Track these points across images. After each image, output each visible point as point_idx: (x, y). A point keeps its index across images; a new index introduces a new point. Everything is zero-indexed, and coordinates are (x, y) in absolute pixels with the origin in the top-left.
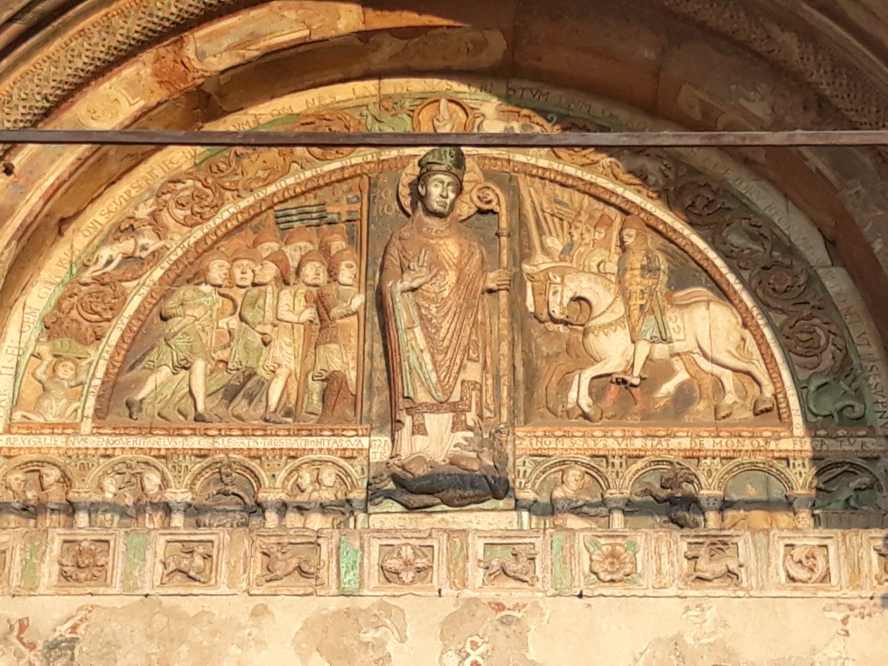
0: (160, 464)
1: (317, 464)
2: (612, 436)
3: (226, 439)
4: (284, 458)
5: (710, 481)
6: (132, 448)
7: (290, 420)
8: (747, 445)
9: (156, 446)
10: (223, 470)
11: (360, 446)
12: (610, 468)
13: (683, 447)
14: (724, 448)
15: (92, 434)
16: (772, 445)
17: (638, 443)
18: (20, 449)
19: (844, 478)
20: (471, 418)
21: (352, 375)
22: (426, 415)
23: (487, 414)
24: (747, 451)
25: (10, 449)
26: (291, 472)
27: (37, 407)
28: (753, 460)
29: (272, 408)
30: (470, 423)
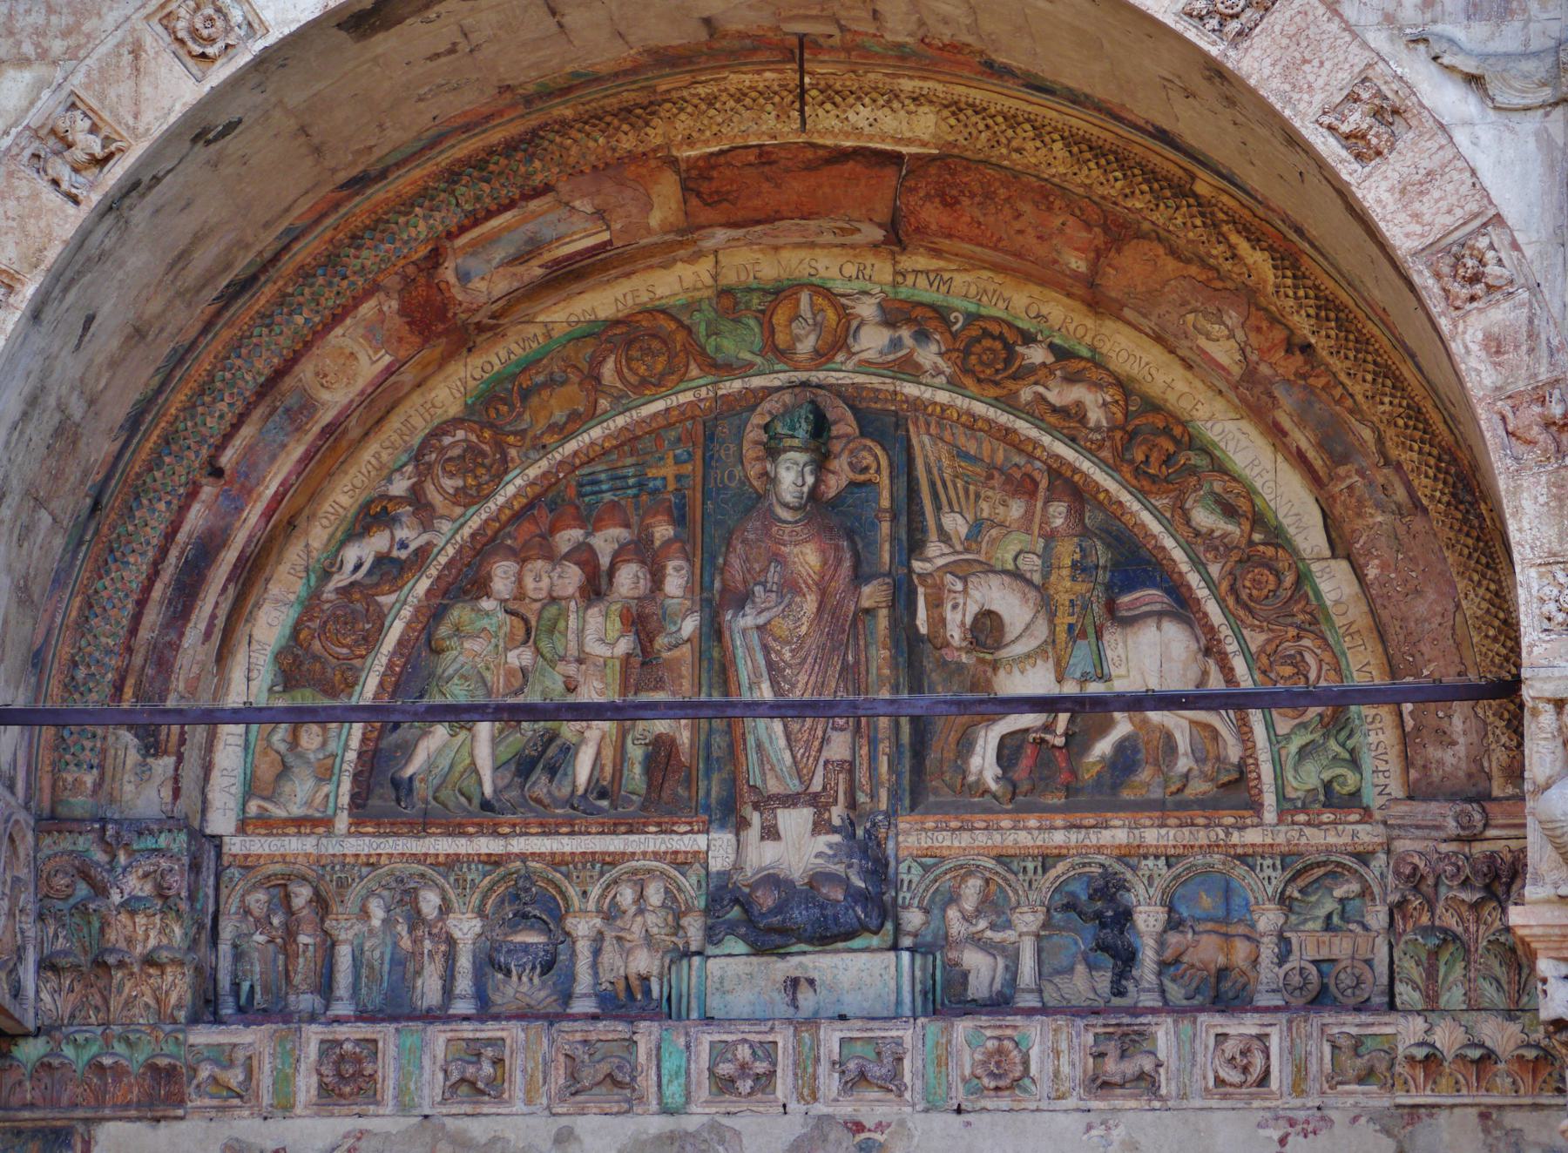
2: (1025, 828)
3: (522, 839)
4: (598, 866)
5: (1151, 891)
6: (403, 854)
7: (605, 803)
8: (1202, 837)
9: (432, 851)
10: (521, 884)
11: (696, 848)
12: (1021, 876)
13: (1117, 842)
14: (1171, 843)
15: (350, 834)
17: (1059, 838)
18: (260, 856)
19: (1328, 882)
20: (837, 814)
22: (779, 811)
23: (862, 798)
24: (1201, 847)
25: (246, 857)
26: (608, 886)
28: (1209, 859)
30: (836, 822)
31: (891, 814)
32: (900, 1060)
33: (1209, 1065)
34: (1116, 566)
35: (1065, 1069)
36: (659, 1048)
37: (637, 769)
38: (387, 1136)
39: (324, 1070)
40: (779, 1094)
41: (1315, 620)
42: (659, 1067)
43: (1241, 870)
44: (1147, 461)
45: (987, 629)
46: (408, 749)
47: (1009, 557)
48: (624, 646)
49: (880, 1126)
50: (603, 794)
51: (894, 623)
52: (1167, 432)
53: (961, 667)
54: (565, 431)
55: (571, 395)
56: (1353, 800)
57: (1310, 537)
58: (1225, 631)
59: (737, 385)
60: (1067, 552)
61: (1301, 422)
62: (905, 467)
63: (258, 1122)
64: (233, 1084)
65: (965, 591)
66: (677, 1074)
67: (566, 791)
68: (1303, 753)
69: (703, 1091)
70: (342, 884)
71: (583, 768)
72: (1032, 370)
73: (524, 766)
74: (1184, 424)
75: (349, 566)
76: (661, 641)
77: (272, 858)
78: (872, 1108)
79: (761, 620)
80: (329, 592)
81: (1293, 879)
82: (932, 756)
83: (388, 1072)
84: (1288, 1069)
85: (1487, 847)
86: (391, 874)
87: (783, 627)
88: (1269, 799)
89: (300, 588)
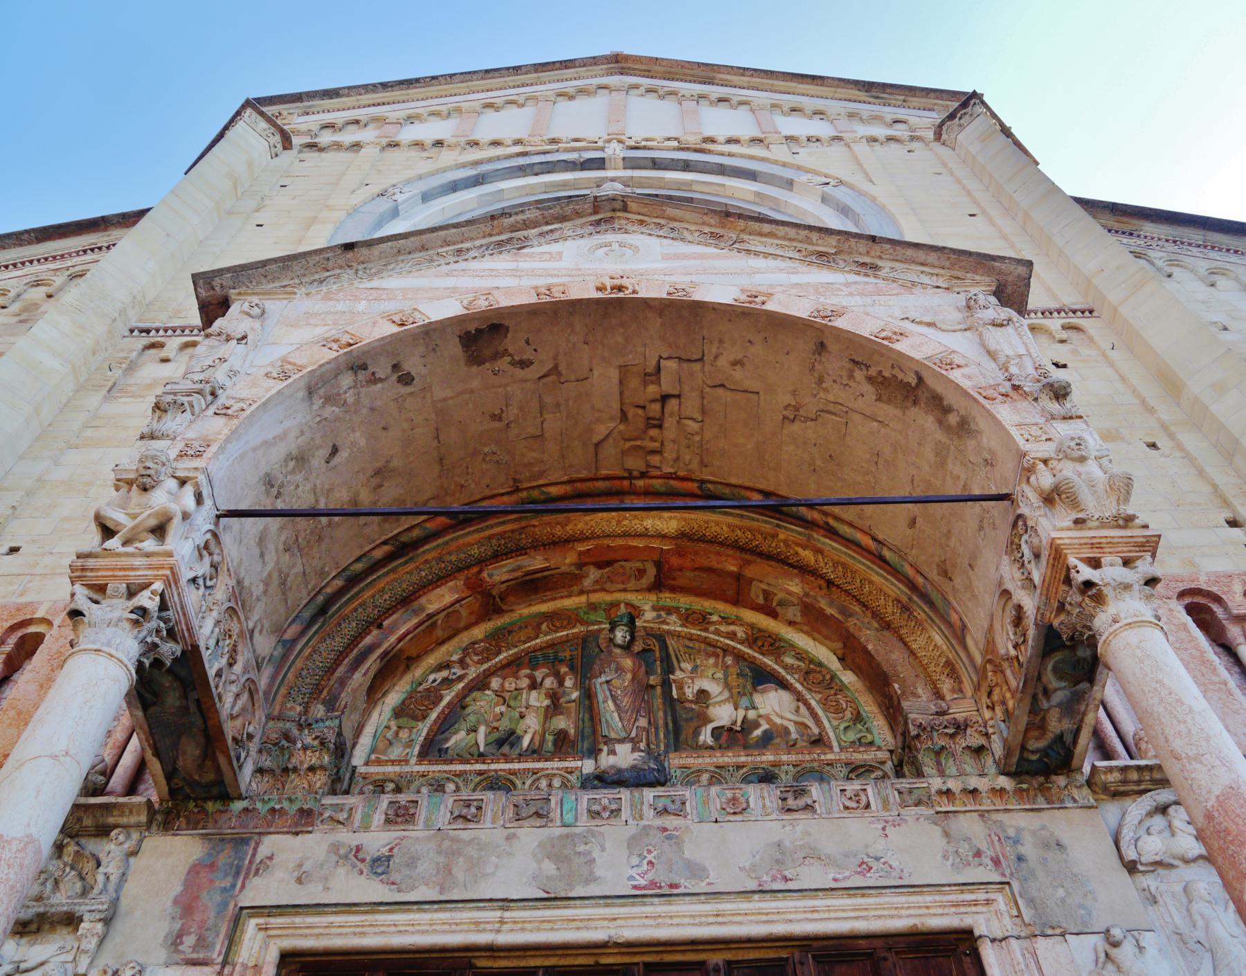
0: (456, 779)
1: (550, 777)
8: (807, 757)
16: (823, 757)
17: (743, 759)
20: (642, 746)
21: (572, 731)
23: (652, 746)
27: (384, 752)
29: (524, 749)
30: (642, 748)
31: (666, 752)
32: (684, 803)
33: (838, 801)
34: (754, 678)
35: (768, 804)
36: (562, 800)
37: (550, 744)
38: (418, 838)
39: (389, 812)
40: (624, 818)
41: (842, 688)
42: (561, 808)
43: (828, 768)
44: (763, 646)
45: (703, 694)
46: (447, 740)
47: (710, 675)
48: (547, 702)
49: (676, 829)
50: (534, 752)
51: (663, 693)
52: (770, 637)
53: (692, 709)
54: (525, 642)
55: (530, 632)
56: (871, 743)
57: (833, 663)
58: (804, 692)
59: (596, 627)
60: (734, 670)
61: (831, 607)
62: (664, 647)
63: (351, 834)
64: (341, 819)
65: (693, 682)
66: (571, 811)
67: (518, 751)
68: (846, 728)
69: (584, 816)
70: (410, 782)
71: (526, 742)
72: (713, 623)
73: (500, 743)
74: (777, 635)
75: (430, 681)
76: (562, 700)
77: (378, 773)
78: (670, 822)
79: (608, 679)
80: (421, 688)
81: (850, 772)
82: (682, 737)
83: (422, 813)
84: (879, 801)
85: (952, 716)
86: (433, 778)
87: (616, 683)
88: (835, 744)
89: (408, 688)
